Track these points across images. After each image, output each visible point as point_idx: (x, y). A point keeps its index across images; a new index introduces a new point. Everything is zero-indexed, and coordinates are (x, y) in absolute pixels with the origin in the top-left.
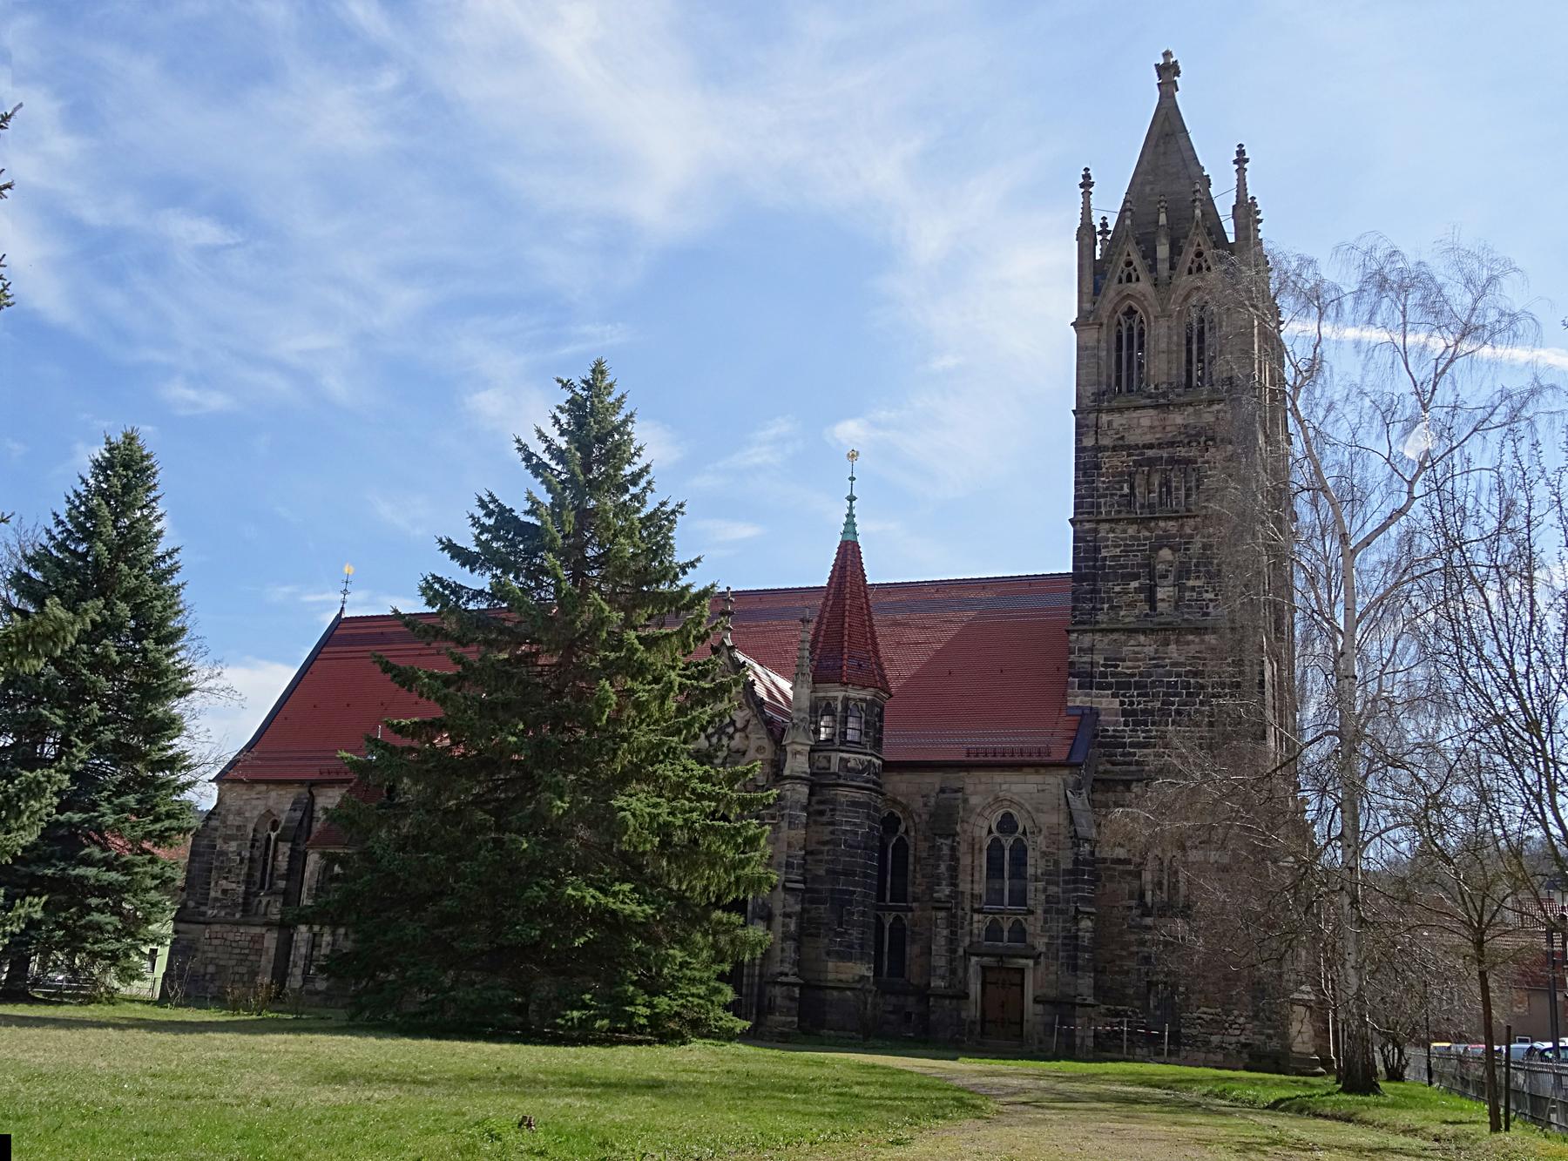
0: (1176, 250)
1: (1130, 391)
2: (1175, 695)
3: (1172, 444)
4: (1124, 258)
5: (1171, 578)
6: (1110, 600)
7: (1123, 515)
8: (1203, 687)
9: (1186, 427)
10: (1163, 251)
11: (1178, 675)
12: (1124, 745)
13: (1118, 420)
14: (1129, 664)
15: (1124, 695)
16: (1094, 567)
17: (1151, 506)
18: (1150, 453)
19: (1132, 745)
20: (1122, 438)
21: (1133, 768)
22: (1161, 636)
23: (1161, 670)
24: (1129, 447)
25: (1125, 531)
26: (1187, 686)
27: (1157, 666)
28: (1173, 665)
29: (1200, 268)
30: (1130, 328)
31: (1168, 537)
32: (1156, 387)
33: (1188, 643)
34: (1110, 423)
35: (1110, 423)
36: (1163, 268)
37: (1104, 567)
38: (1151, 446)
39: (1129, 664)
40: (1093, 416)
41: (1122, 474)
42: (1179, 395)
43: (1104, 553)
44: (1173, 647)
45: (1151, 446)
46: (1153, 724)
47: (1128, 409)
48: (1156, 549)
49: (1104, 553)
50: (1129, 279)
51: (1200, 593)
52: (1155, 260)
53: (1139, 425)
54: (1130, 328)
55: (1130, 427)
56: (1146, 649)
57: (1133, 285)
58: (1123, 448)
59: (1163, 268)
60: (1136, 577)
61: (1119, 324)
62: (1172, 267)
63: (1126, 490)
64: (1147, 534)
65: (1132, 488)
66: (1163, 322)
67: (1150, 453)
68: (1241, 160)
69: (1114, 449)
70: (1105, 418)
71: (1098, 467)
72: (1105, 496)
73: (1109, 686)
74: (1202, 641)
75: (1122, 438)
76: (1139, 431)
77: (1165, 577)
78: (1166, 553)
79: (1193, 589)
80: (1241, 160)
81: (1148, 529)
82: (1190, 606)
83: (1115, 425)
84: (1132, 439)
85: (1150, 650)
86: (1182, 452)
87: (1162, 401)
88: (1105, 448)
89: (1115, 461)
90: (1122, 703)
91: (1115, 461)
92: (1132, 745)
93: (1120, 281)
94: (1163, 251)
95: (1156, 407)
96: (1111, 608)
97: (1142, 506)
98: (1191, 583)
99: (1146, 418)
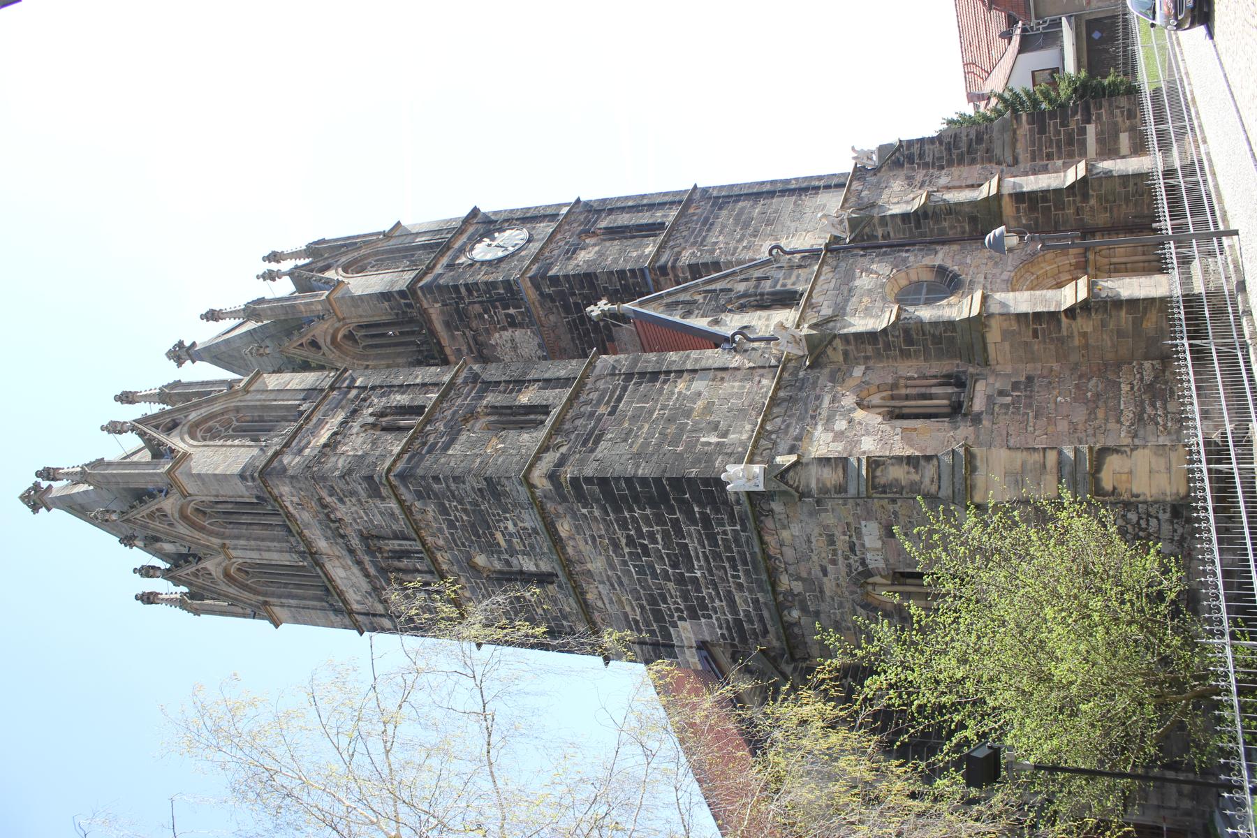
2: (652, 567)
8: (628, 537)
11: (625, 563)
12: (738, 622)
15: (672, 616)
18: (372, 571)
19: (734, 611)
21: (766, 614)
23: (625, 580)
27: (621, 584)
28: (613, 568)
39: (628, 609)
73: (664, 630)
74: (572, 538)
79: (509, 542)
85: (604, 589)
90: (681, 618)
92: (734, 611)
96: (565, 618)
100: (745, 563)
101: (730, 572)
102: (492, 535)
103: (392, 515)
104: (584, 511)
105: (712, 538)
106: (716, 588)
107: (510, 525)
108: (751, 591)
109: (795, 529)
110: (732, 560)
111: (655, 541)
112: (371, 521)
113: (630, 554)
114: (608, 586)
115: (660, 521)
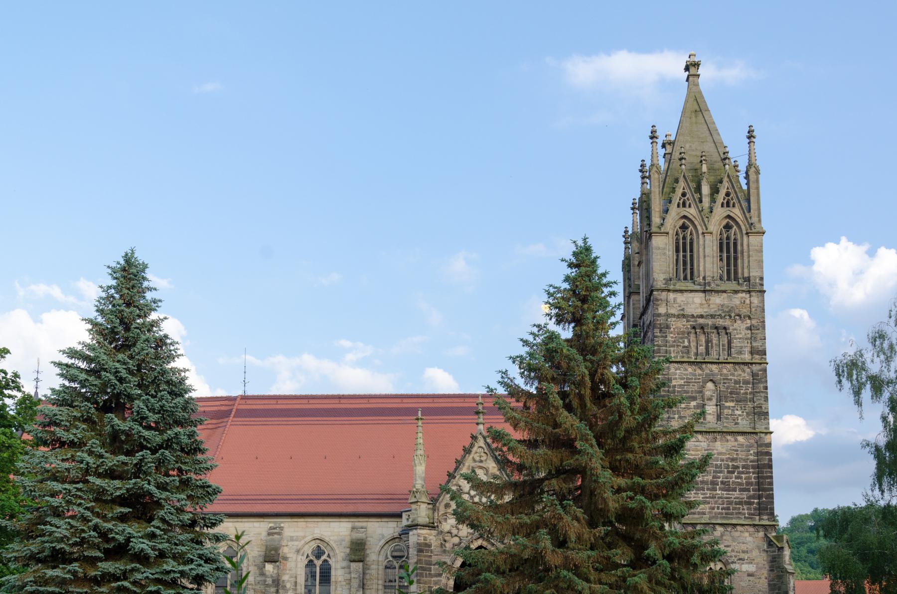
0: (715, 191)
1: (685, 278)
2: (721, 472)
3: (712, 316)
4: (681, 191)
5: (714, 401)
6: (679, 412)
7: (685, 359)
8: (738, 467)
9: (722, 306)
10: (706, 189)
11: (722, 460)
13: (680, 298)
14: (693, 453)
16: (668, 391)
17: (701, 354)
18: (701, 321)
20: (683, 310)
21: (696, 516)
22: (711, 436)
24: (688, 316)
25: (686, 370)
26: (728, 467)
28: (719, 454)
29: (728, 203)
30: (684, 238)
31: (713, 375)
32: (704, 278)
33: (727, 441)
34: (675, 299)
35: (675, 299)
36: (706, 201)
37: (674, 392)
38: (702, 316)
40: (664, 293)
41: (683, 333)
42: (717, 285)
43: (674, 383)
44: (718, 444)
45: (702, 316)
46: (708, 489)
47: (686, 291)
48: (705, 382)
49: (674, 383)
50: (684, 205)
51: (733, 410)
52: (701, 194)
53: (693, 303)
54: (684, 238)
55: (688, 303)
56: (702, 444)
57: (687, 209)
58: (684, 316)
59: (706, 201)
60: (694, 399)
61: (677, 234)
62: (713, 200)
63: (686, 344)
64: (700, 372)
65: (689, 342)
66: (708, 237)
67: (701, 321)
68: (751, 136)
69: (678, 316)
70: (672, 296)
71: (668, 327)
72: (673, 346)
74: (736, 440)
75: (683, 310)
76: (693, 306)
77: (710, 399)
78: (710, 385)
79: (729, 408)
80: (751, 136)
81: (701, 369)
82: (727, 418)
83: (679, 300)
84: (689, 311)
85: (704, 445)
86: (720, 322)
87: (708, 288)
88: (674, 316)
89: (679, 324)
91: (679, 324)
93: (678, 206)
94: (706, 189)
95: (704, 291)
96: (680, 417)
97: (697, 354)
98: (727, 404)
99: (698, 298)
100: (726, 514)
101: (721, 506)
102: (733, 401)
103: (740, 353)
104: (752, 452)
105: (740, 503)
106: (710, 497)
107: (739, 412)
108: (710, 512)
109: (749, 539)
110: (728, 509)
111: (737, 478)
112: (736, 339)
113: (728, 465)
114: (706, 447)
115: (748, 484)
